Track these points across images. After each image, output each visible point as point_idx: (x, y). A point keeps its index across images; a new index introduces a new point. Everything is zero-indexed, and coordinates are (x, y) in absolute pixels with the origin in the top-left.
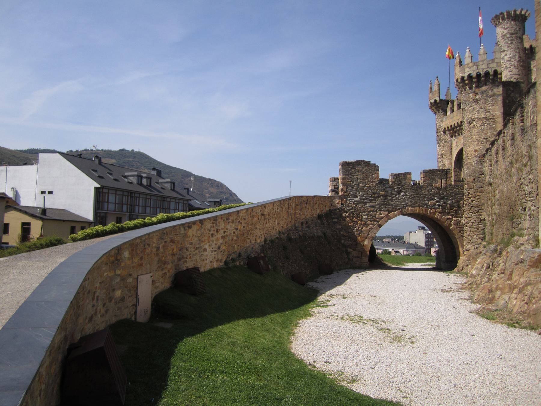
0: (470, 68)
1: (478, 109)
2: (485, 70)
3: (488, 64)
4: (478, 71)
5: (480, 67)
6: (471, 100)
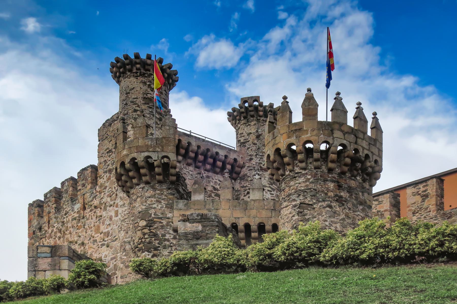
0: (345, 133)
1: (343, 216)
2: (366, 152)
3: (370, 144)
4: (356, 146)
5: (359, 141)
6: (331, 194)
